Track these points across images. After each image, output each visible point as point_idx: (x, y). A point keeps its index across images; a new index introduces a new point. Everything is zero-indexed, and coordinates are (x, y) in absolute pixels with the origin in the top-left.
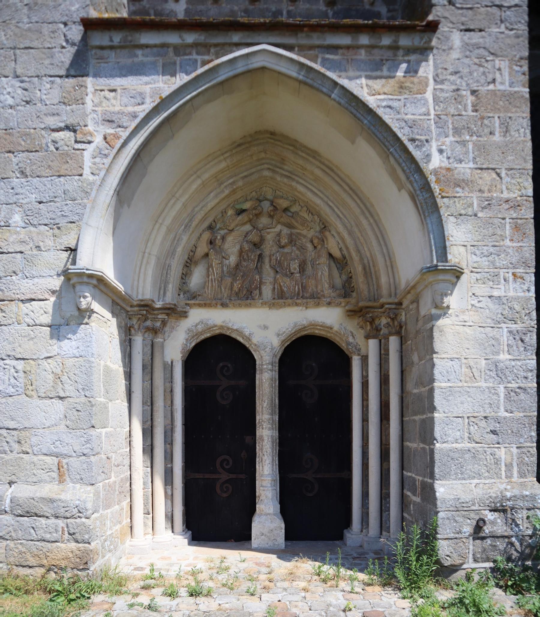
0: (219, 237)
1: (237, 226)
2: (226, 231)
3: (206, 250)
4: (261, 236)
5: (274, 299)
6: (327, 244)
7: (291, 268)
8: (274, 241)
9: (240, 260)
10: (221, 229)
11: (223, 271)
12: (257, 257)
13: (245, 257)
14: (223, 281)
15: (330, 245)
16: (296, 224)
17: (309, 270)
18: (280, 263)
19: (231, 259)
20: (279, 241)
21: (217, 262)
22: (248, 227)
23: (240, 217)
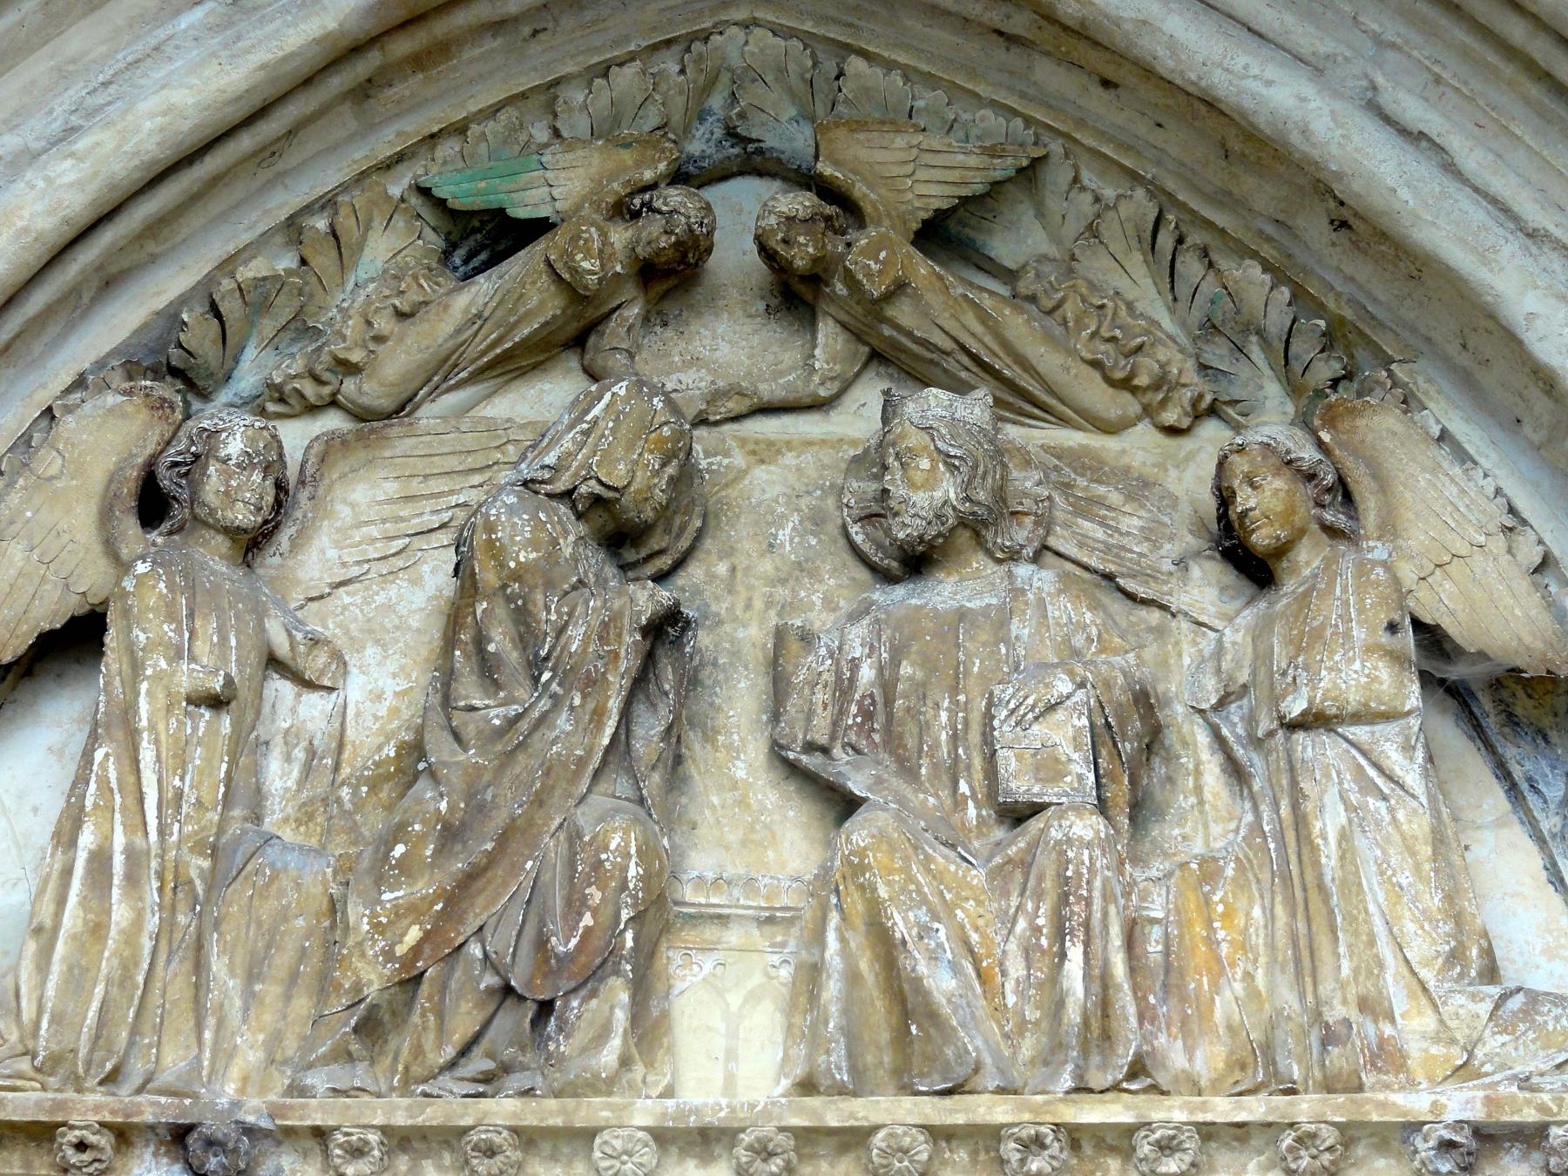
0: (234, 447)
1: (442, 373)
2: (333, 421)
3: (90, 578)
4: (685, 476)
5: (807, 1086)
6: (1389, 529)
7: (1008, 762)
8: (816, 520)
9: (446, 680)
10: (278, 400)
11: (242, 792)
12: (631, 638)
13: (500, 641)
14: (239, 894)
15: (1418, 536)
16: (1048, 360)
17: (1204, 812)
18: (884, 721)
19: (355, 689)
20: (878, 512)
21: (187, 678)
22: (549, 396)
23: (484, 287)
